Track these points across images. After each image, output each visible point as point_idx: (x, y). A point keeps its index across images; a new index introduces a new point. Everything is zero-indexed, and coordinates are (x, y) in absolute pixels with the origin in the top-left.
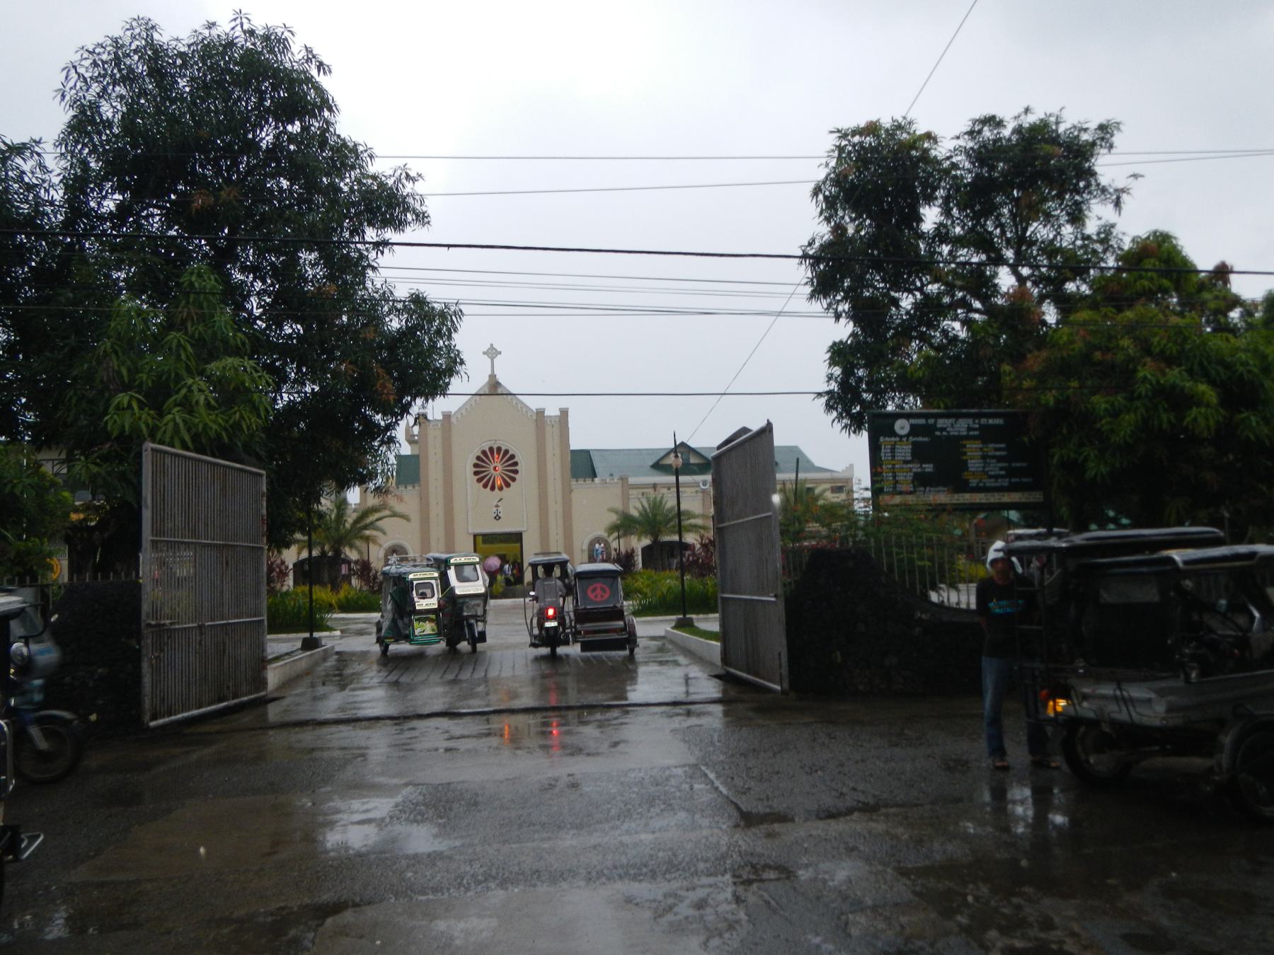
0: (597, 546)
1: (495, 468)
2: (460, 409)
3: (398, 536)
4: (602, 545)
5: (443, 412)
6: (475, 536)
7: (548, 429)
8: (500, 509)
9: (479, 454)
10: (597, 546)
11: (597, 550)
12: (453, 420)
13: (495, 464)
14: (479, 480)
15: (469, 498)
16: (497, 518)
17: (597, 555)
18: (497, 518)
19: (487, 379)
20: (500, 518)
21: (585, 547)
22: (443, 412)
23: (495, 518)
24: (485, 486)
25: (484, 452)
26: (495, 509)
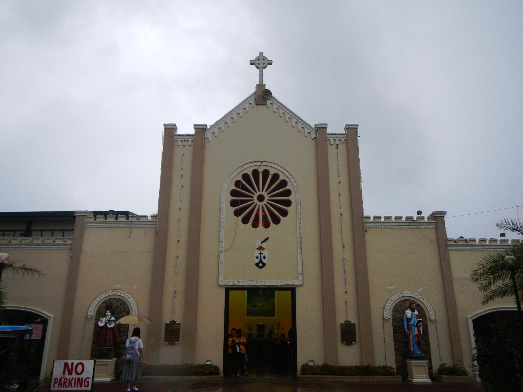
0: (409, 313)
1: (261, 198)
2: (217, 123)
3: (119, 286)
4: (416, 312)
5: (195, 125)
6: (228, 290)
7: (331, 150)
8: (265, 253)
9: (239, 178)
10: (409, 313)
11: (409, 320)
12: (208, 135)
13: (260, 193)
14: (237, 213)
15: (222, 234)
16: (261, 265)
17: (409, 328)
18: (261, 265)
19: (253, 90)
20: (264, 265)
21: (388, 314)
22: (195, 125)
23: (257, 265)
24: (245, 221)
25: (245, 177)
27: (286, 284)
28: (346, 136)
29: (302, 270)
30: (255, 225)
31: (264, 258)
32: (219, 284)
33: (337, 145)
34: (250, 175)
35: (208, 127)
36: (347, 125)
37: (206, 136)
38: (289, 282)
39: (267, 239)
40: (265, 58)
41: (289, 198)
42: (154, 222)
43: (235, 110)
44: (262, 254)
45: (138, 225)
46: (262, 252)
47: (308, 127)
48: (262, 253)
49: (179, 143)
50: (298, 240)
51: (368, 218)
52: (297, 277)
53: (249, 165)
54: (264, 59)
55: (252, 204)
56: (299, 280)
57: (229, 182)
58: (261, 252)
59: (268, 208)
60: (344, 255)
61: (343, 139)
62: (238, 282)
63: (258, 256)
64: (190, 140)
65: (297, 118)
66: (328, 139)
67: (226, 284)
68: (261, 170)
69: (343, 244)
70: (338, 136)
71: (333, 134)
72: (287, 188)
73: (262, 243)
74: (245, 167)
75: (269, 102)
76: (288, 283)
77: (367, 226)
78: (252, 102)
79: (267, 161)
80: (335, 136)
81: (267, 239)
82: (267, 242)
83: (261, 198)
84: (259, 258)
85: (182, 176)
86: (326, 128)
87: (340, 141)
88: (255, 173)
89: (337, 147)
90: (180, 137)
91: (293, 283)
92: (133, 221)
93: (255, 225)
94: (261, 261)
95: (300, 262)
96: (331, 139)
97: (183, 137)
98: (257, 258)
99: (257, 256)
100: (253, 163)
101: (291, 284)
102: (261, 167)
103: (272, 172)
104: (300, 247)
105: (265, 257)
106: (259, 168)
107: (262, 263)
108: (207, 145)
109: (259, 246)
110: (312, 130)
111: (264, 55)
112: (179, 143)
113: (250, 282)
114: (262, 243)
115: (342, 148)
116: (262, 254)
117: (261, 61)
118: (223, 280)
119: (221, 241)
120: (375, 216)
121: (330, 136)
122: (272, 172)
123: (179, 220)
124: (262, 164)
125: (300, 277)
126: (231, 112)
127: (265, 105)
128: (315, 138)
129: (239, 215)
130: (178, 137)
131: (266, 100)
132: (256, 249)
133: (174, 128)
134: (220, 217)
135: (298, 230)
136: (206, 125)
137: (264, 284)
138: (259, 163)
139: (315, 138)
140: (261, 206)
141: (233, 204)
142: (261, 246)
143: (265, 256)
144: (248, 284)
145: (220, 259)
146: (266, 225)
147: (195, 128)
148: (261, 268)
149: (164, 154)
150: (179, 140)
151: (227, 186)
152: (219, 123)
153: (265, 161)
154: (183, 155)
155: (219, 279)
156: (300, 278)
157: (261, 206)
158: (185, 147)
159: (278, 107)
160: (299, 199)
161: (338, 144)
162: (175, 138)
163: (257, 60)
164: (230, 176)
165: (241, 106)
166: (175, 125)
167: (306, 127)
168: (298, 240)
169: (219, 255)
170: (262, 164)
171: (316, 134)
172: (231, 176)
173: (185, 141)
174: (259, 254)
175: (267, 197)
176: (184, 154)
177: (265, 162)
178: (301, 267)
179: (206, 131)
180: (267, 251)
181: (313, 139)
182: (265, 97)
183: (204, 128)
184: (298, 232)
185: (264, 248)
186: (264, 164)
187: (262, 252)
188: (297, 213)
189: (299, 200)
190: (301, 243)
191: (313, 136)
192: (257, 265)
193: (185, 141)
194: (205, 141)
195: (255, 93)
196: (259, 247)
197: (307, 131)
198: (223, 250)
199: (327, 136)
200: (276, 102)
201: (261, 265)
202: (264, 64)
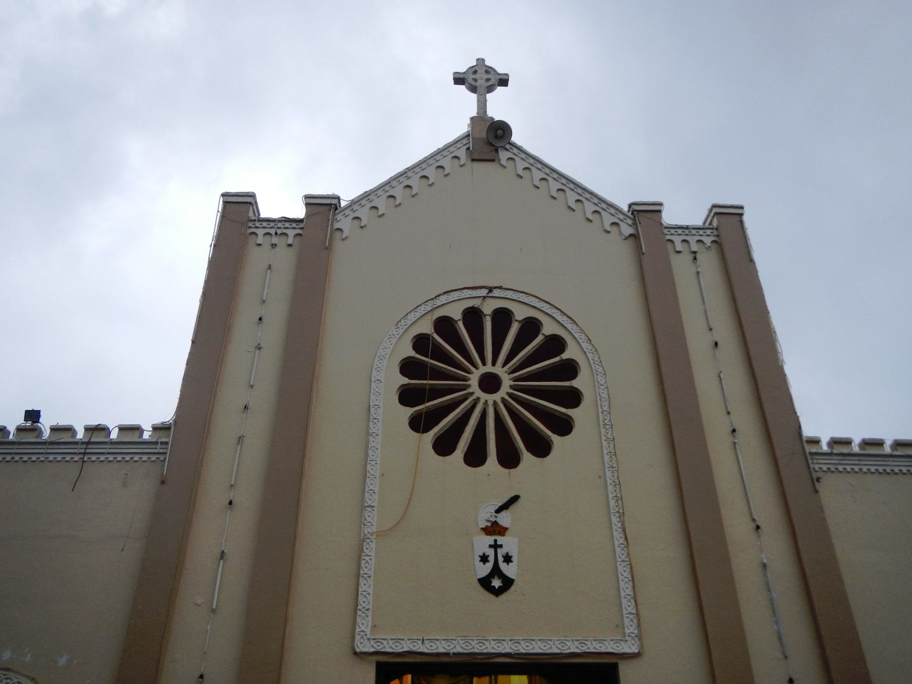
1: (490, 383)
2: (366, 196)
7: (681, 266)
8: (509, 543)
9: (426, 327)
12: (344, 223)
15: (373, 484)
20: (508, 583)
23: (485, 582)
24: (444, 446)
25: (444, 325)
26: (483, 543)
27: (584, 649)
28: (715, 232)
29: (633, 601)
30: (475, 457)
31: (508, 559)
32: (358, 650)
33: (695, 253)
34: (456, 322)
35: (343, 204)
36: (714, 206)
37: (337, 225)
38: (594, 643)
39: (515, 499)
40: (490, 70)
41: (575, 383)
42: (159, 446)
43: (417, 170)
44: (501, 546)
45: (108, 453)
46: (501, 540)
47: (612, 211)
48: (499, 543)
49: (260, 240)
50: (612, 503)
51: (816, 442)
52: (621, 626)
53: (455, 296)
54: (487, 72)
55: (465, 398)
56: (627, 638)
57: (398, 337)
58: (496, 541)
59: (512, 411)
60: (763, 556)
61: (708, 241)
62: (420, 642)
63: (487, 554)
64: (291, 233)
65: (580, 191)
66: (668, 237)
67: (379, 648)
68: (488, 308)
69: (754, 520)
70: (694, 232)
71: (681, 227)
72: (565, 356)
73: (498, 511)
74: (443, 299)
75: (503, 155)
76: (593, 647)
77: (817, 467)
78: (462, 153)
79: (504, 286)
80: (687, 232)
81: (515, 499)
82: (512, 508)
83: (490, 383)
84: (492, 559)
85: (260, 319)
86: (660, 211)
87: (700, 244)
88: (473, 316)
89: (695, 258)
90: (265, 224)
91: (609, 647)
92: (92, 440)
93: (475, 457)
94: (496, 571)
95: (625, 575)
96: (677, 240)
97: (272, 224)
98: (484, 559)
99: (484, 554)
100: (466, 290)
101: (603, 650)
102: (488, 301)
103: (520, 313)
104: (619, 525)
105: (511, 557)
106: (482, 304)
107: (499, 578)
108: (339, 247)
109: (488, 521)
110: (622, 217)
111: (487, 63)
112: (260, 240)
113: (461, 642)
114: (498, 511)
115: (709, 262)
116: (501, 546)
117: (482, 83)
118: (368, 637)
119: (366, 505)
120: (835, 438)
121: (672, 231)
122: (520, 313)
123: (240, 440)
124: (491, 295)
125: (631, 628)
126: (406, 172)
127: (493, 160)
128: (634, 236)
129: (426, 430)
130: (258, 224)
131: (497, 151)
132: (483, 533)
133: (250, 203)
134: (368, 434)
135: (609, 474)
136: (338, 198)
137: (508, 650)
138: (484, 292)
139: (631, 235)
140: (490, 403)
141: (407, 397)
142: (495, 524)
143: (510, 554)
144: (455, 651)
145: (363, 562)
146: (509, 459)
147: (307, 205)
148: (497, 592)
149: (213, 264)
150: (260, 232)
151: (391, 347)
152: (372, 197)
153: (500, 288)
154: (270, 267)
155: (358, 630)
156: (632, 629)
157: (490, 403)
158: (276, 250)
159: (528, 166)
160: (602, 385)
161: (696, 249)
162: (250, 227)
163: (471, 72)
164: (400, 321)
165: (431, 161)
166: (252, 196)
167: (605, 210)
168: (612, 503)
169: (361, 550)
170: (491, 295)
171: (635, 225)
172: (403, 322)
173: (276, 233)
174: (491, 546)
175: (507, 382)
176: (272, 267)
177: (499, 290)
178: (629, 591)
179: (337, 211)
180: (516, 539)
181: (626, 238)
182: (494, 144)
183: (331, 204)
184: (609, 482)
185: (506, 529)
186: (496, 293)
187: (501, 540)
188: (602, 423)
189: (602, 387)
190: (622, 515)
191: (627, 230)
192: (485, 582)
193: (276, 233)
194: (331, 237)
195: (467, 136)
196: (489, 524)
197: (608, 219)
198: (372, 534)
199: (666, 231)
200: (523, 156)
201: (496, 583)
202: (488, 80)
